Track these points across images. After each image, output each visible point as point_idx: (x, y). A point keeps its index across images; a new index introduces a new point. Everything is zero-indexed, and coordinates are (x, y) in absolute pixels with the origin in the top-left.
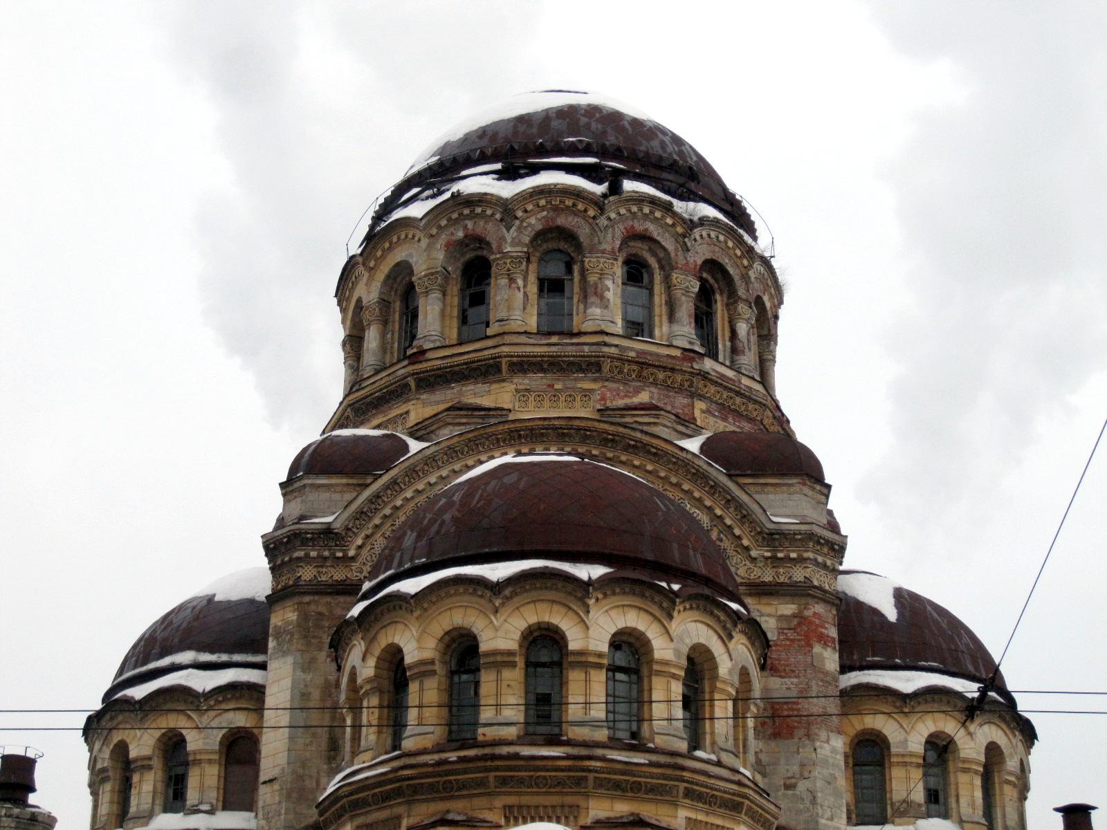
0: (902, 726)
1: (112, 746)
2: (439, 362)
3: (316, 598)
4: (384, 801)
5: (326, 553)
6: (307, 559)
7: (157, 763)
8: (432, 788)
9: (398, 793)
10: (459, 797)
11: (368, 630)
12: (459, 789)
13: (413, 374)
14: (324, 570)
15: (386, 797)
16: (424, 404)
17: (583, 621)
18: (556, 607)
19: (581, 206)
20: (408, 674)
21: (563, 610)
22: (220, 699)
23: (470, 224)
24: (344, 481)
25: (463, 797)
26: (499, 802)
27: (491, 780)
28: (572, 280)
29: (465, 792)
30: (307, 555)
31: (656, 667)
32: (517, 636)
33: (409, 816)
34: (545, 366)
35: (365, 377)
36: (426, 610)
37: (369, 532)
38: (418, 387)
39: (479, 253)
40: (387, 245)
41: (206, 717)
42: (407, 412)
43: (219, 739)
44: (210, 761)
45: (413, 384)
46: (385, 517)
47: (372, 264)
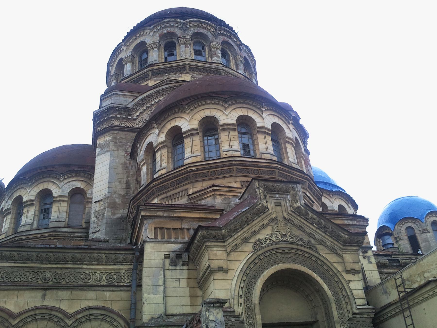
0: (330, 201)
3: (120, 132)
5: (124, 116)
6: (116, 118)
7: (37, 203)
9: (187, 179)
11: (160, 124)
13: (151, 70)
14: (123, 123)
15: (180, 182)
17: (261, 116)
18: (249, 110)
19: (209, 28)
20: (184, 136)
21: (253, 112)
22: (70, 176)
23: (169, 29)
24: (130, 94)
26: (239, 179)
27: (235, 169)
28: (205, 51)
30: (116, 116)
31: (287, 140)
32: (236, 119)
33: (193, 188)
34: (202, 70)
36: (192, 110)
37: (142, 111)
38: (152, 75)
39: (171, 40)
40: (134, 38)
41: (62, 183)
43: (68, 192)
44: (63, 201)
45: (150, 74)
46: (148, 107)
47: (128, 44)
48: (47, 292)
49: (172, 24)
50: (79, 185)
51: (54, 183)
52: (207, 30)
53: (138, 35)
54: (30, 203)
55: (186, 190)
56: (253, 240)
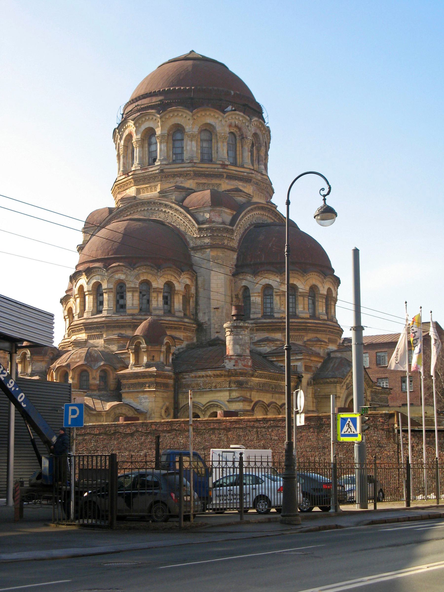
1: (140, 280)
2: (235, 172)
4: (297, 330)
5: (230, 236)
8: (313, 330)
9: (303, 329)
10: (319, 334)
12: (320, 332)
15: (298, 330)
16: (228, 184)
25: (320, 334)
26: (328, 336)
29: (321, 333)
35: (195, 161)
38: (226, 178)
42: (220, 184)
48: (273, 395)
49: (241, 119)
50: (188, 282)
51: (175, 277)
52: (261, 130)
53: (208, 113)
54: (157, 290)
55: (302, 336)
56: (346, 383)
